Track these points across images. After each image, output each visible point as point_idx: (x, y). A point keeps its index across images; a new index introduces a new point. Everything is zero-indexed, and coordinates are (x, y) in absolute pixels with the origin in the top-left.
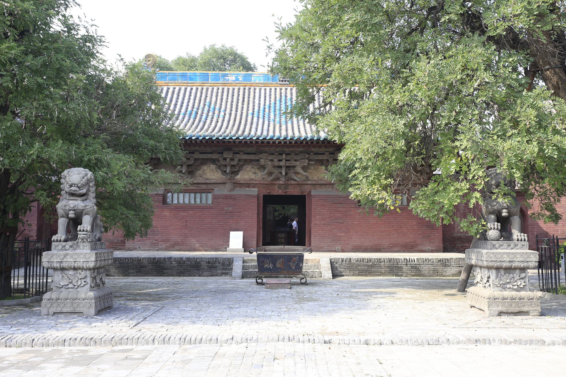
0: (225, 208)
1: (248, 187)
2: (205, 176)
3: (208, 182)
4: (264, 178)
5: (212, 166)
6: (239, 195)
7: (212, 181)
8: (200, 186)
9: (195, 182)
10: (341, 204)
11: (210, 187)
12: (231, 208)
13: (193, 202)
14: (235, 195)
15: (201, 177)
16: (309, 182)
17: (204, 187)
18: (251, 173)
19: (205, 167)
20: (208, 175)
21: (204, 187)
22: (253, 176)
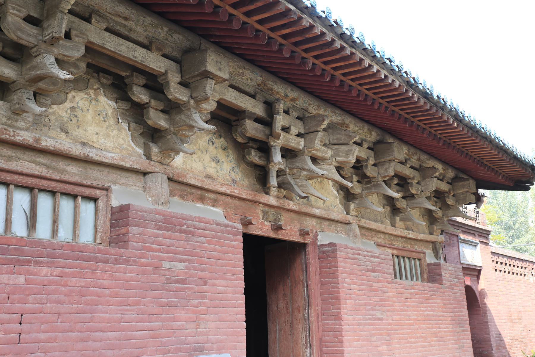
0: (166, 265)
1: (202, 199)
2: (79, 133)
3: (94, 155)
4: (234, 181)
5: (103, 99)
6: (200, 220)
7: (109, 157)
8: (61, 164)
9: (47, 143)
10: (374, 271)
11: (96, 176)
12: (181, 266)
13: (20, 229)
14: (192, 219)
15: (64, 130)
16: (317, 212)
17: (73, 172)
18: (207, 158)
19: (79, 99)
20: (91, 129)
21: (73, 172)
22: (212, 169)
